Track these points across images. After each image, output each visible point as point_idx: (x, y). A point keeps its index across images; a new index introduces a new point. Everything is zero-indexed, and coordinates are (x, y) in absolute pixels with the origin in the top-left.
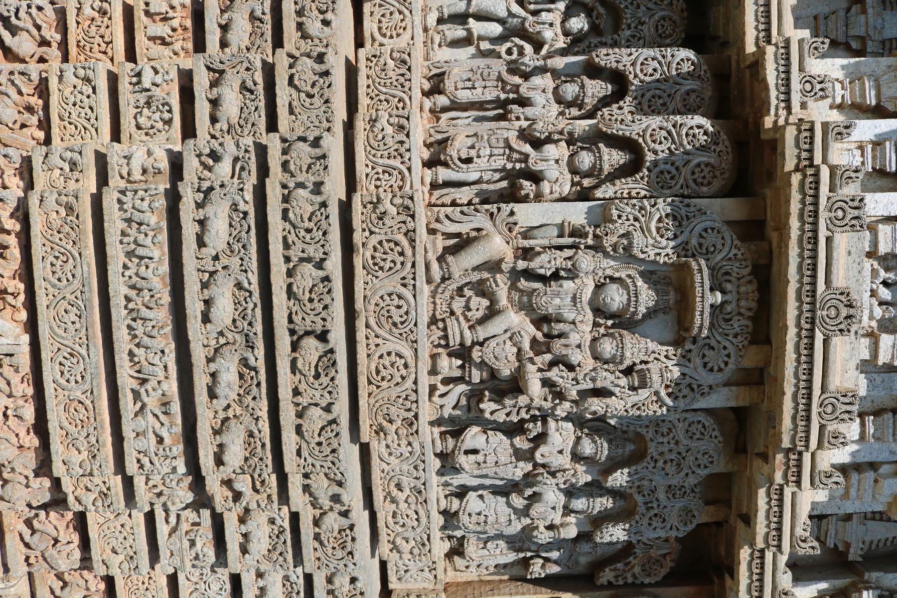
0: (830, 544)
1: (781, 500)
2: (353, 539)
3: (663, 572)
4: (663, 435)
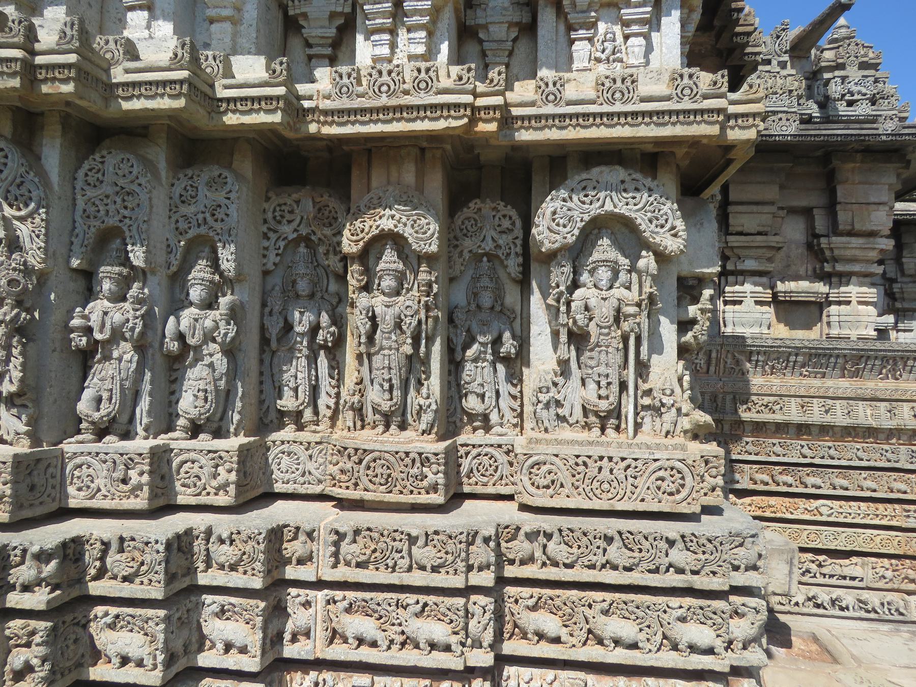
0: (332, 32)
1: (134, 85)
2: (133, 539)
3: (334, 203)
4: (99, 211)
